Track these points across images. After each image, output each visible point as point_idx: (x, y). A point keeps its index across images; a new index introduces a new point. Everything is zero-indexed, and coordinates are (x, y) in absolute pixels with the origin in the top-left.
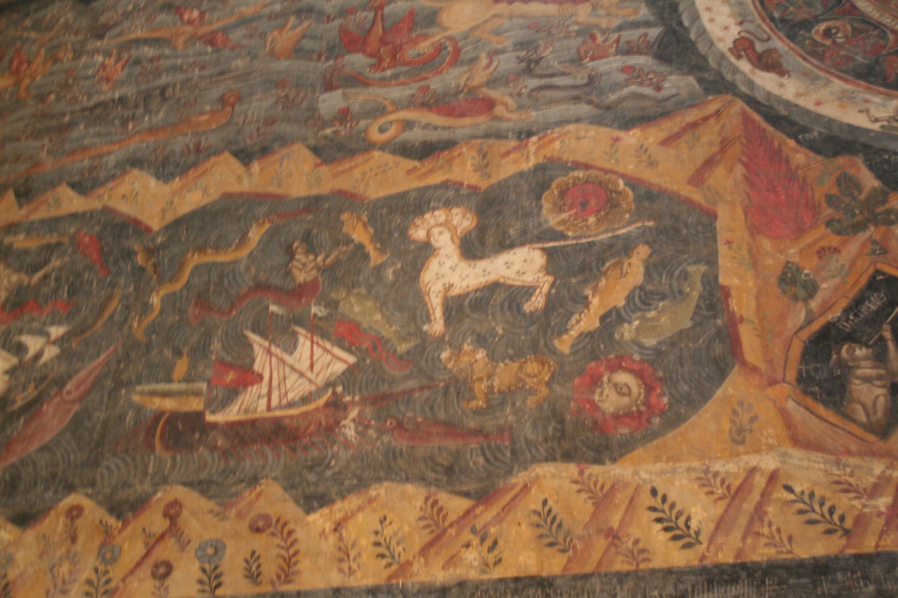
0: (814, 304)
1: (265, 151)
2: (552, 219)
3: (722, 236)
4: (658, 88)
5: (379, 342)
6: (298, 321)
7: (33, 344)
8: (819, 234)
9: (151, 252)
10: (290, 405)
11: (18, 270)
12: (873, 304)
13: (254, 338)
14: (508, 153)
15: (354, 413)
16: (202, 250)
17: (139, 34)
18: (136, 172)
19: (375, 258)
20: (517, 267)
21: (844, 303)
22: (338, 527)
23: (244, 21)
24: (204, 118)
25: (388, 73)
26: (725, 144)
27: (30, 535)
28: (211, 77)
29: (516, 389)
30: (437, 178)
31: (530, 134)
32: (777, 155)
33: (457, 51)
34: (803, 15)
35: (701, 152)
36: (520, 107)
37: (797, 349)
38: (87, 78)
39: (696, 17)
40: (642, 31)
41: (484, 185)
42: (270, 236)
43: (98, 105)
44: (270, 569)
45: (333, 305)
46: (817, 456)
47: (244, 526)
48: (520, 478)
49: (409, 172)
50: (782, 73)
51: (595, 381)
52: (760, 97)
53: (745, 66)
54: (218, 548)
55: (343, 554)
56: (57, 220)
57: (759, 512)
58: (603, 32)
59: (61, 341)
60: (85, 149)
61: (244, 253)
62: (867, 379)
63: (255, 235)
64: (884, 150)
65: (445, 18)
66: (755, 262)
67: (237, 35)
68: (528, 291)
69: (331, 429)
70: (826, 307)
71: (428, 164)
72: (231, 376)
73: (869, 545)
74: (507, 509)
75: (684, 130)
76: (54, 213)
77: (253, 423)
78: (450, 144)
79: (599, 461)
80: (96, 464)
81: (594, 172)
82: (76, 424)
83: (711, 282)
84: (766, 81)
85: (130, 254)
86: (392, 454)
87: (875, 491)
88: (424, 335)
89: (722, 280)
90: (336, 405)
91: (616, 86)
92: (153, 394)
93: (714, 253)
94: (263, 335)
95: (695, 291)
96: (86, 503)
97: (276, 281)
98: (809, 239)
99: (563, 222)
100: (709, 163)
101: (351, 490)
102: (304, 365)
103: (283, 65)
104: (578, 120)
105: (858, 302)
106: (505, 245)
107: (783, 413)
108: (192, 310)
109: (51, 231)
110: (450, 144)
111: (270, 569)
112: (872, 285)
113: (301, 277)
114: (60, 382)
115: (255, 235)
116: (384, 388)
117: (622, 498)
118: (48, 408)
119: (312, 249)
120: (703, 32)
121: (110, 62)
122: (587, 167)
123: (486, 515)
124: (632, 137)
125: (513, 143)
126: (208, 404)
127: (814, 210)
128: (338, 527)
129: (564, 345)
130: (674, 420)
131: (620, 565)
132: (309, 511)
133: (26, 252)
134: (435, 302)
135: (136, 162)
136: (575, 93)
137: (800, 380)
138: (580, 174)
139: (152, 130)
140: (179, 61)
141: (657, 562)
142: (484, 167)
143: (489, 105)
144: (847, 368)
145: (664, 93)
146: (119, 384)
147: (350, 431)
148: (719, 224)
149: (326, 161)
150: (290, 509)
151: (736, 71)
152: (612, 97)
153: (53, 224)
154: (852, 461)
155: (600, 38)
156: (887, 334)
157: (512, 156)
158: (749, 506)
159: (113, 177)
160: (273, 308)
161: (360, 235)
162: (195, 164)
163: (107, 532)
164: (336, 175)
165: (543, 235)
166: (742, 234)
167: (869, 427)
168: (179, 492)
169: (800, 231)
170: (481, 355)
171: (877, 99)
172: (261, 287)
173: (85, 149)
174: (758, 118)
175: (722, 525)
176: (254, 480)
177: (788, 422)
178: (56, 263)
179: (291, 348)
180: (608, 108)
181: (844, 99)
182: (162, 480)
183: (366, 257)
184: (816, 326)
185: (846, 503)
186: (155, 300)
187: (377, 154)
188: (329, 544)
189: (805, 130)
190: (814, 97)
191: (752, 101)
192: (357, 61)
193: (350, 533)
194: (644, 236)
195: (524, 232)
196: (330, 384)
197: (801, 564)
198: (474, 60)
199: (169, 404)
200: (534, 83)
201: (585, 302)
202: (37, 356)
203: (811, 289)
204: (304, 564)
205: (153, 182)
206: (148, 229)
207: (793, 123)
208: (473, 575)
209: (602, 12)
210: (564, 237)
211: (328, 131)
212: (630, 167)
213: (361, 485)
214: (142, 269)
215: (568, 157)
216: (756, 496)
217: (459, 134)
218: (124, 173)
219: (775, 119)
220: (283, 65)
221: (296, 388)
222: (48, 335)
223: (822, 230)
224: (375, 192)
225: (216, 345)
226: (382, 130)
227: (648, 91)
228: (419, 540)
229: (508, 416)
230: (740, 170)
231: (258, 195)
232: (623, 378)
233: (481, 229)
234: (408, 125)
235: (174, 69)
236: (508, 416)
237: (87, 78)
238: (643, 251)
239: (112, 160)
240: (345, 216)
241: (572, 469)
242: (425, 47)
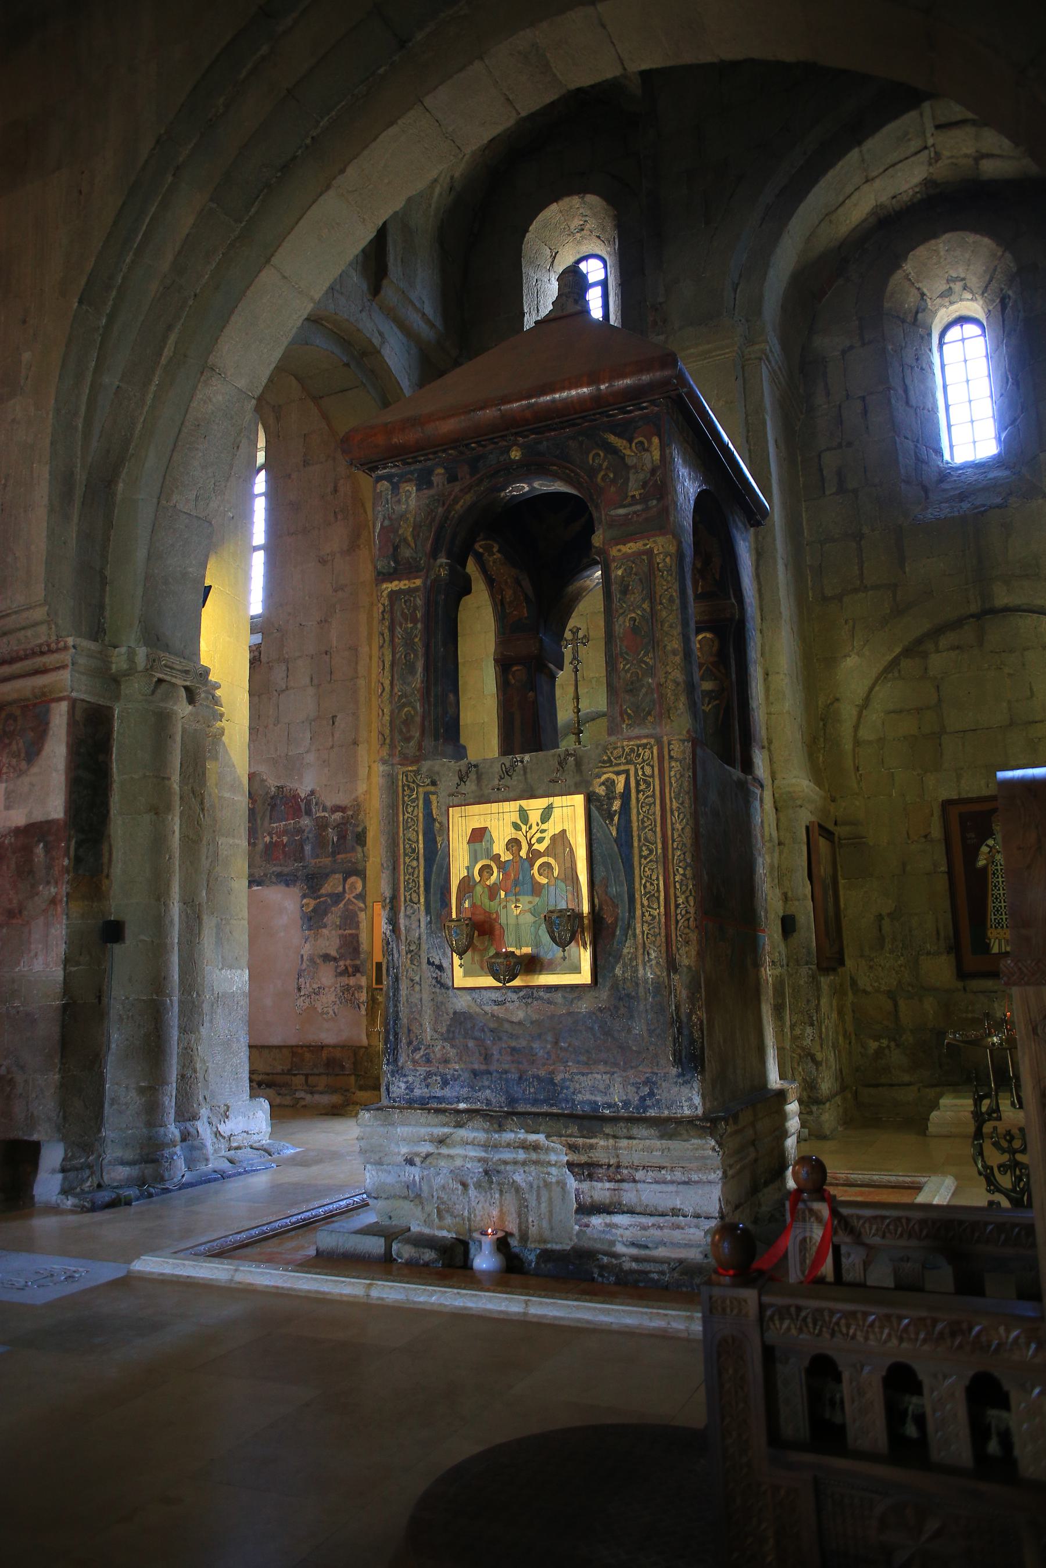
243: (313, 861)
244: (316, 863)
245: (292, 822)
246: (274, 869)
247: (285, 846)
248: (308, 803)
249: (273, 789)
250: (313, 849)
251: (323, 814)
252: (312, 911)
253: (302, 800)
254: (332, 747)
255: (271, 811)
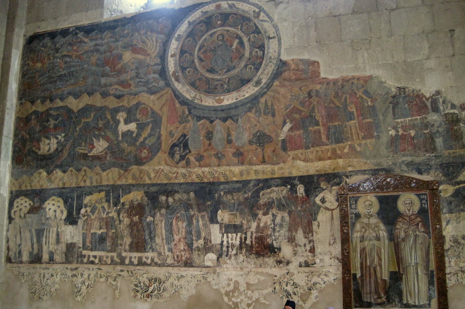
0: (173, 139)
1: (92, 94)
2: (138, 116)
3: (163, 123)
4: (158, 84)
5: (112, 141)
6: (100, 135)
7: (60, 137)
8: (177, 124)
9: (76, 118)
10: (100, 153)
11: (54, 120)
12: (181, 140)
13: (94, 139)
14: (132, 100)
15: (109, 155)
16: (84, 118)
17: (65, 53)
18: (70, 96)
19: (112, 123)
20: (132, 127)
21: (177, 139)
22: (107, 174)
23: (86, 52)
24: (81, 82)
25: (113, 73)
26: (167, 100)
27: (66, 174)
28: (81, 70)
29: (130, 152)
30: (121, 104)
31: (136, 95)
32: (174, 105)
33: (125, 68)
34: (186, 66)
35: (163, 102)
36: (135, 87)
37: (169, 147)
38: (57, 66)
39: (167, 64)
40: (158, 66)
41: (128, 107)
42: (95, 115)
43: (61, 75)
44: (99, 181)
45: (105, 132)
46: (168, 167)
47: (95, 174)
48: (131, 168)
49: (117, 102)
50: (179, 82)
51: (141, 151)
52: (174, 89)
53: (173, 79)
54: (92, 178)
55: (108, 180)
56: (58, 107)
57: (159, 176)
58: (151, 66)
59: (64, 137)
60: (60, 88)
61: (90, 120)
62: (177, 154)
63: (92, 115)
64: (191, 105)
65: (124, 57)
66: (166, 130)
67: (85, 56)
68: (132, 133)
69: (106, 157)
70: (175, 139)
71: (119, 101)
72: (91, 146)
73: (172, 182)
74: (129, 173)
75: (161, 97)
76: (58, 106)
77: (95, 156)
78: (123, 96)
79: (141, 166)
80: (73, 162)
81: (145, 106)
82: (69, 154)
83: (160, 132)
84: (176, 84)
85: (72, 118)
86: (114, 163)
87: (174, 173)
88: (118, 140)
89: (161, 133)
90: (106, 153)
91: (152, 83)
92: (80, 149)
93: (161, 126)
94: (95, 138)
95: (157, 134)
96: (73, 169)
97: (96, 127)
98: (175, 125)
99: (140, 117)
100: (163, 105)
101: (108, 169)
102: (101, 145)
103: (94, 68)
104: (144, 92)
105: (179, 139)
106: (131, 122)
107: (165, 159)
108: (84, 132)
109: (58, 110)
110: (123, 96)
111: (99, 181)
112: (182, 136)
113: (100, 126)
114: (65, 146)
115: (92, 115)
116: (113, 150)
117: (143, 172)
118: (64, 151)
119: (101, 120)
120: (168, 68)
121: (61, 61)
122: (144, 104)
123: (126, 174)
124: (152, 97)
125: (133, 97)
126: (89, 151)
127: (177, 118)
128: (107, 174)
129: (138, 144)
130: (151, 159)
131: (142, 183)
132: (103, 172)
133: (54, 115)
134: (120, 133)
135: (69, 94)
136: (144, 84)
137: (169, 153)
138: (143, 106)
139: (72, 85)
140: (74, 64)
141: (146, 183)
142: (128, 102)
143: (130, 85)
144: (175, 151)
145: (159, 86)
146: (75, 147)
147: (108, 158)
148: (163, 120)
149: (103, 98)
150: (101, 172)
151: (172, 81)
152: (150, 86)
153: (58, 108)
154: (173, 168)
155: (150, 68)
156: (182, 146)
157: (133, 100)
158: (158, 174)
159: (66, 97)
160: (96, 132)
161: (109, 117)
162: (80, 96)
163: (77, 175)
164: (105, 101)
165: (136, 120)
166: (166, 122)
167: (176, 162)
168: (85, 168)
169: (174, 123)
170: (126, 145)
171: (192, 92)
172: (94, 127)
173: (60, 88)
174: (173, 94)
175: (155, 177)
176: (96, 166)
177: (166, 161)
178: (60, 119)
179: (99, 142)
180: (150, 89)
181: (188, 91)
182: (83, 166)
183: (110, 122)
184: (173, 143)
185: (171, 175)
186: (78, 129)
187: (111, 97)
188: (106, 178)
189: (180, 98)
190: (183, 90)
191: (173, 90)
192: (107, 68)
193: (109, 176)
194: (151, 122)
195: (134, 119)
196: (105, 149)
197: (163, 184)
198: (128, 72)
199: (82, 151)
200: (138, 80)
201: (141, 135)
202: (61, 140)
203: (174, 135)
204: (103, 181)
205: (74, 100)
206: (74, 112)
207: (178, 97)
208: (124, 183)
209: (151, 60)
210: (139, 121)
211: (103, 89)
212: (151, 105)
213: (110, 168)
214: (74, 121)
215: (142, 101)
216: (159, 173)
217: (125, 93)
218: (68, 96)
219: (175, 95)
220: (94, 68)
221: (101, 149)
222: (61, 135)
223: (178, 123)
224: (111, 107)
225: (88, 140)
226: (112, 91)
227: (156, 85)
228: (118, 177)
229: (129, 157)
230: (168, 107)
231: (92, 105)
232: (145, 151)
233: (127, 117)
234: (116, 89)
235: (74, 66)
236: (129, 157)
237: (57, 66)
238: (151, 125)
239: (65, 92)
240: (106, 112)
241: (137, 167)
242: (119, 66)
243: (446, 153)
244: (449, 153)
245: (418, 117)
246: (404, 159)
247: (413, 138)
248: (434, 102)
249: (393, 89)
250: (445, 141)
251: (452, 111)
252: (452, 196)
253: (427, 99)
254: (453, 55)
255: (394, 108)
